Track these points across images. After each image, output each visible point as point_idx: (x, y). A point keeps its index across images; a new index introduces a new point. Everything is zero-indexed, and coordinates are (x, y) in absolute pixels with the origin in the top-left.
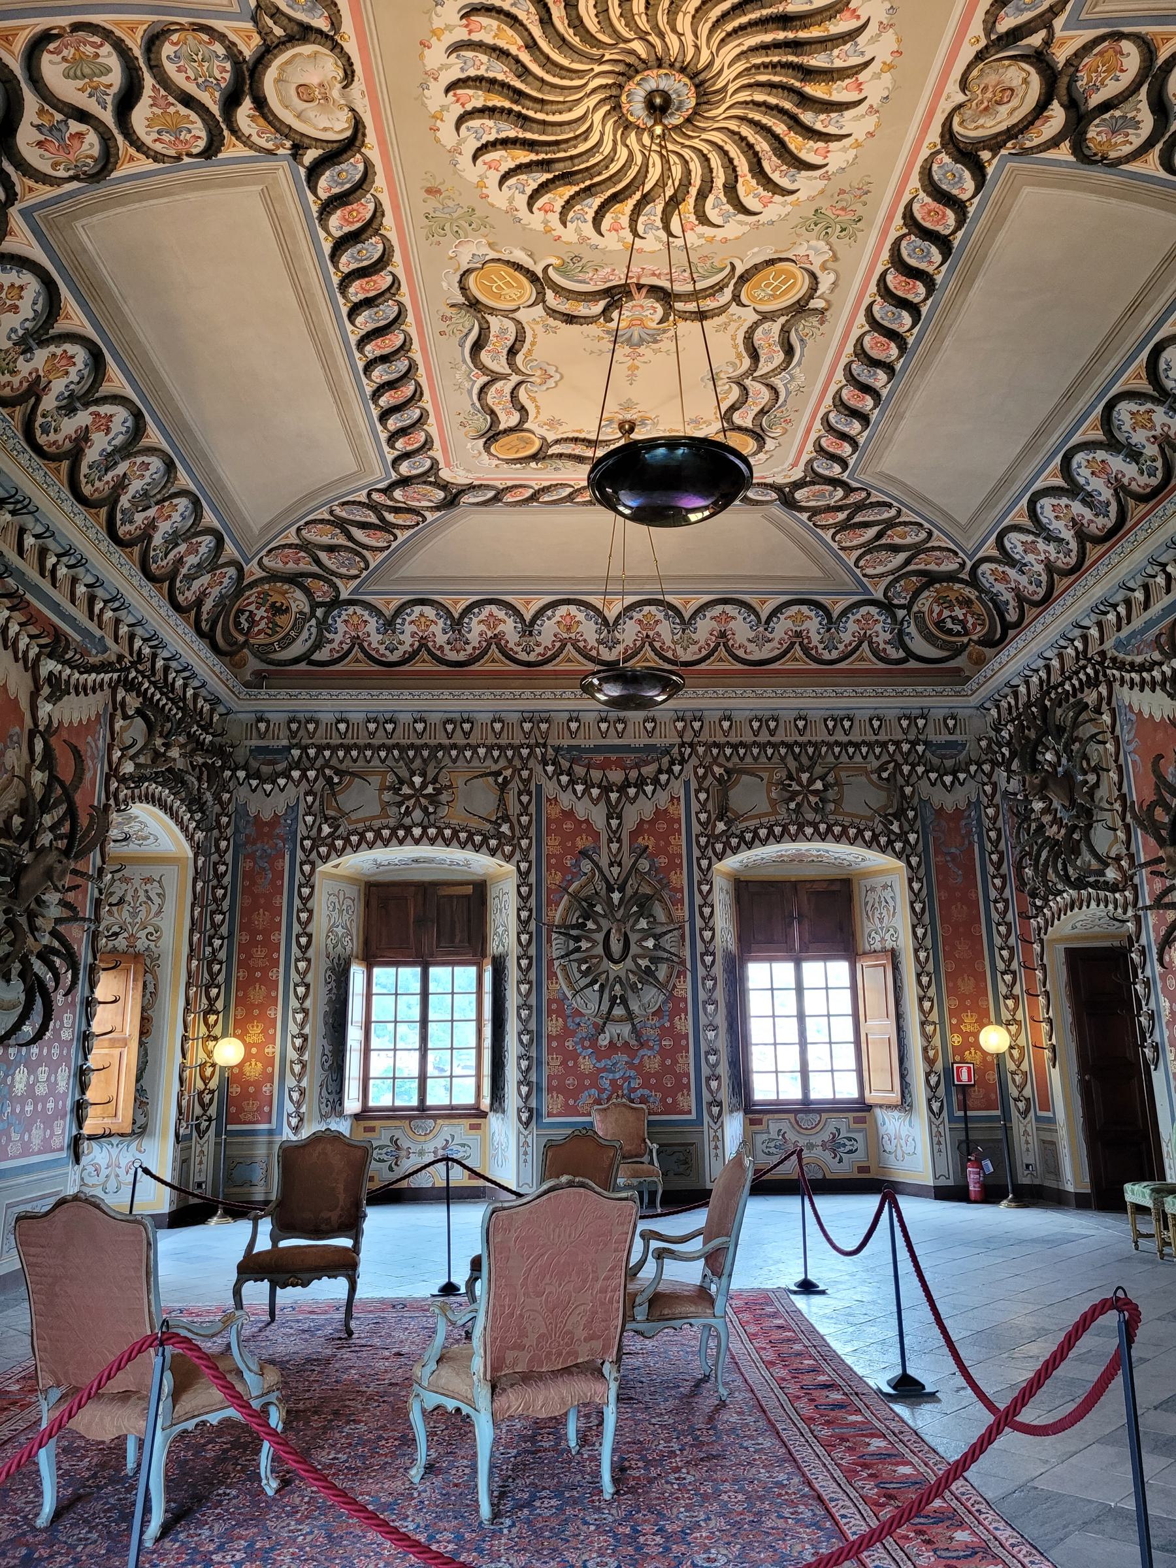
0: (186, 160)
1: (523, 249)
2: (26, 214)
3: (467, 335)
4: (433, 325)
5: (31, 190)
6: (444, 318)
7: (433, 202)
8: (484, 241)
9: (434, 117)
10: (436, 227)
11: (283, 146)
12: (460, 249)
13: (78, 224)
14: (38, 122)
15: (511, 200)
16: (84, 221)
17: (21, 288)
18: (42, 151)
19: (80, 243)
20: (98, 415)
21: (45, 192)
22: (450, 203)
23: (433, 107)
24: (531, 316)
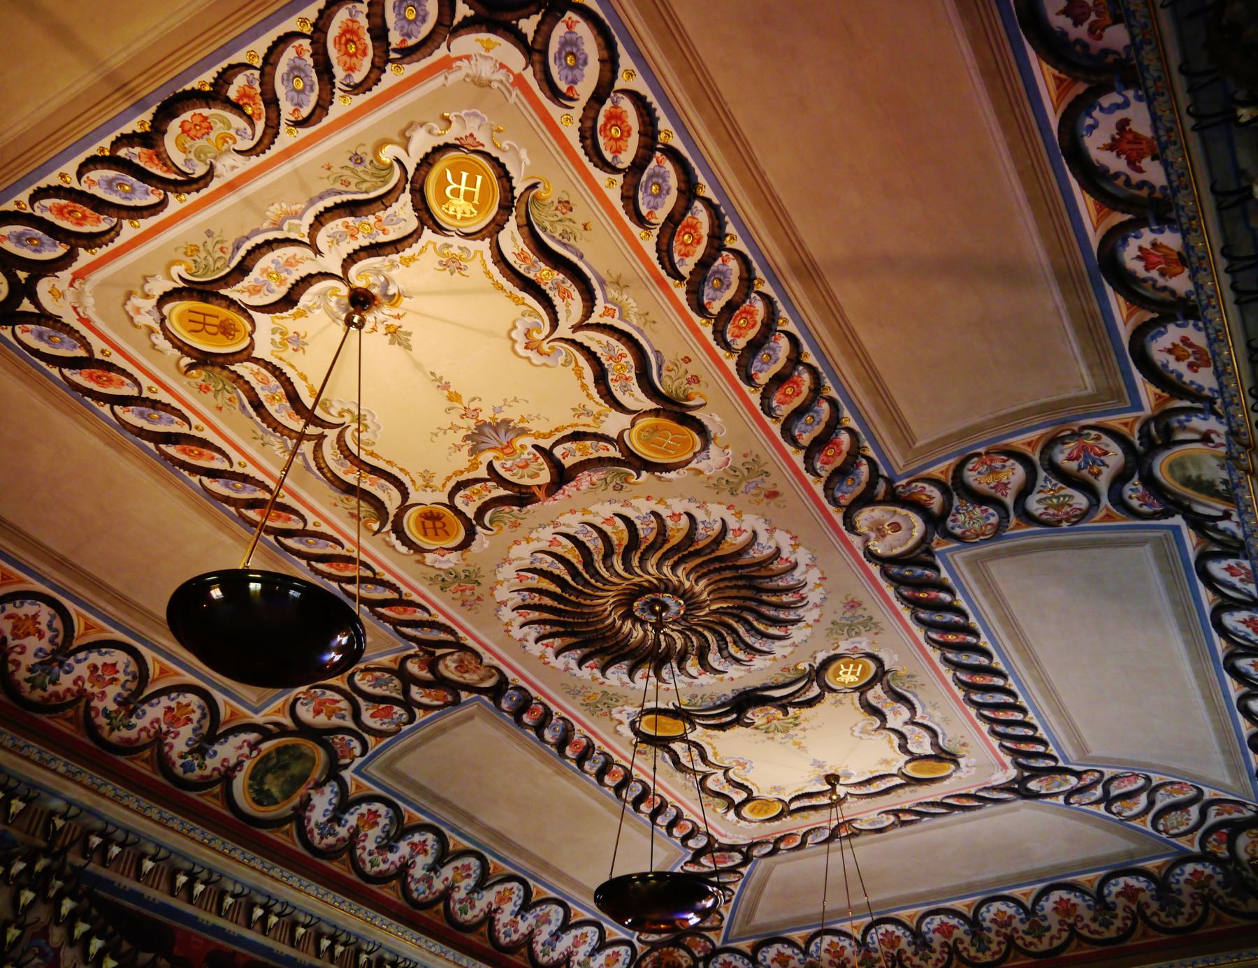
0: (982, 450)
1: (670, 481)
2: (1139, 407)
3: (660, 368)
4: (701, 364)
5: (1126, 424)
6: (695, 380)
7: (768, 485)
8: (707, 473)
9: (797, 545)
10: (753, 468)
11: (903, 487)
12: (724, 459)
13: (1090, 391)
14: (1102, 468)
15: (708, 513)
16: (1084, 393)
17: (1170, 351)
18: (1106, 449)
19: (1093, 375)
20: (1132, 163)
21: (1113, 421)
22: (753, 491)
23: (801, 550)
24: (614, 423)
